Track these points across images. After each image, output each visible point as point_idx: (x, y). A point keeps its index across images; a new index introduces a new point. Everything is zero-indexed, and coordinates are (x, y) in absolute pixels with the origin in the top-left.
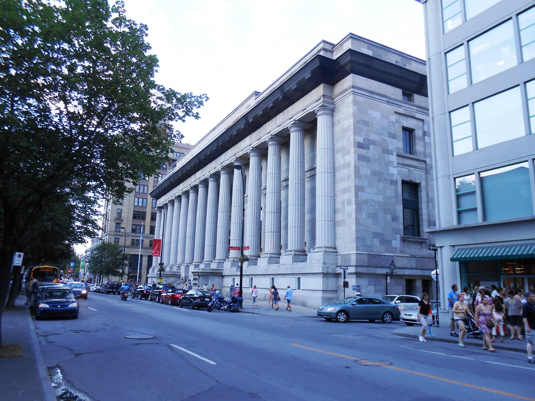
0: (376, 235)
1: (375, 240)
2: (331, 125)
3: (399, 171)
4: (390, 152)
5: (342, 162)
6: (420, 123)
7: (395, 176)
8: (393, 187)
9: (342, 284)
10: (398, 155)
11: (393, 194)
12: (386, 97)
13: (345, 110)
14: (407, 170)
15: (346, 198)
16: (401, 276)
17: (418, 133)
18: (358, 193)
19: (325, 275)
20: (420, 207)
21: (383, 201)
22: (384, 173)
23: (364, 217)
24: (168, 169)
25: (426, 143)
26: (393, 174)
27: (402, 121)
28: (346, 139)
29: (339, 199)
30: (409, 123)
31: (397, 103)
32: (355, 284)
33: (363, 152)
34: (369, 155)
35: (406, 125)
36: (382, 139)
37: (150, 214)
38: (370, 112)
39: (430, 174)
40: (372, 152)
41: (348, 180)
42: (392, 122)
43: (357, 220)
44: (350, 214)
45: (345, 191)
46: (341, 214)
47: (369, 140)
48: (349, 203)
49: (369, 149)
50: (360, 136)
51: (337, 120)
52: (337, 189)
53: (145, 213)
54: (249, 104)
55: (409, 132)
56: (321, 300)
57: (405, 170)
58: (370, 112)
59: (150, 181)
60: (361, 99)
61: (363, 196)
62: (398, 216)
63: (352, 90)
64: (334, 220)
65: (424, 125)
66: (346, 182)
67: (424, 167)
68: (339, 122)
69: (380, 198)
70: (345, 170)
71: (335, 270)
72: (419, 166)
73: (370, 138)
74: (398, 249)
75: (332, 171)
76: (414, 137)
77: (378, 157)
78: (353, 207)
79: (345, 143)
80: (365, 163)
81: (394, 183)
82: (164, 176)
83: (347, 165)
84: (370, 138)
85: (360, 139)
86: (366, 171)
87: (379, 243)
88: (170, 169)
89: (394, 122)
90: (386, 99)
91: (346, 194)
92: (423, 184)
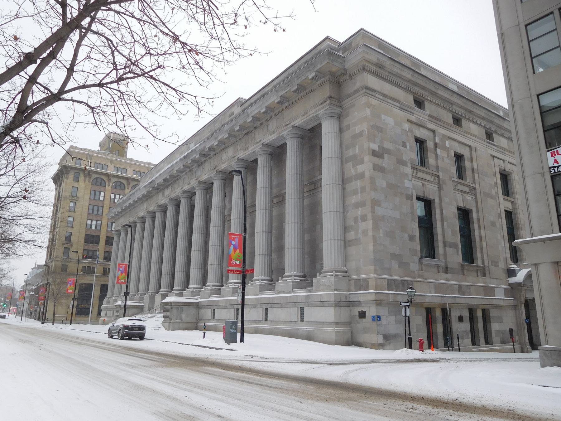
0: (394, 256)
1: (393, 261)
2: (338, 131)
3: (413, 185)
4: (404, 163)
5: (353, 172)
6: (431, 134)
7: (410, 190)
8: (409, 202)
9: (358, 314)
10: (412, 168)
13: (356, 113)
14: (421, 184)
15: (359, 213)
16: (421, 305)
17: (430, 145)
19: (338, 304)
20: (434, 226)
21: (399, 217)
22: (399, 186)
23: (381, 235)
24: (126, 189)
26: (409, 188)
28: (357, 147)
29: (351, 214)
30: (422, 133)
31: (409, 110)
32: (374, 315)
33: (378, 161)
34: (384, 165)
35: (418, 136)
36: (396, 148)
37: (105, 238)
38: (383, 117)
40: (387, 162)
41: (361, 193)
42: (405, 130)
44: (365, 232)
45: (358, 205)
46: (353, 233)
47: (383, 148)
48: (364, 218)
49: (384, 158)
50: (374, 142)
51: (346, 126)
52: (347, 203)
53: (99, 237)
54: (233, 111)
55: (421, 142)
56: (334, 333)
57: (419, 184)
58: (383, 117)
59: (105, 202)
60: (374, 101)
61: (380, 211)
62: (415, 236)
63: (364, 91)
65: (435, 136)
66: (359, 195)
67: (437, 182)
68: (348, 127)
69: (397, 215)
72: (432, 180)
73: (385, 146)
74: (416, 272)
77: (393, 168)
78: (369, 224)
79: (357, 151)
80: (380, 173)
81: (409, 197)
82: (121, 196)
83: (361, 176)
85: (374, 147)
86: (381, 183)
88: (128, 189)
89: (407, 130)
90: (399, 105)
91: (360, 209)
92: (437, 201)
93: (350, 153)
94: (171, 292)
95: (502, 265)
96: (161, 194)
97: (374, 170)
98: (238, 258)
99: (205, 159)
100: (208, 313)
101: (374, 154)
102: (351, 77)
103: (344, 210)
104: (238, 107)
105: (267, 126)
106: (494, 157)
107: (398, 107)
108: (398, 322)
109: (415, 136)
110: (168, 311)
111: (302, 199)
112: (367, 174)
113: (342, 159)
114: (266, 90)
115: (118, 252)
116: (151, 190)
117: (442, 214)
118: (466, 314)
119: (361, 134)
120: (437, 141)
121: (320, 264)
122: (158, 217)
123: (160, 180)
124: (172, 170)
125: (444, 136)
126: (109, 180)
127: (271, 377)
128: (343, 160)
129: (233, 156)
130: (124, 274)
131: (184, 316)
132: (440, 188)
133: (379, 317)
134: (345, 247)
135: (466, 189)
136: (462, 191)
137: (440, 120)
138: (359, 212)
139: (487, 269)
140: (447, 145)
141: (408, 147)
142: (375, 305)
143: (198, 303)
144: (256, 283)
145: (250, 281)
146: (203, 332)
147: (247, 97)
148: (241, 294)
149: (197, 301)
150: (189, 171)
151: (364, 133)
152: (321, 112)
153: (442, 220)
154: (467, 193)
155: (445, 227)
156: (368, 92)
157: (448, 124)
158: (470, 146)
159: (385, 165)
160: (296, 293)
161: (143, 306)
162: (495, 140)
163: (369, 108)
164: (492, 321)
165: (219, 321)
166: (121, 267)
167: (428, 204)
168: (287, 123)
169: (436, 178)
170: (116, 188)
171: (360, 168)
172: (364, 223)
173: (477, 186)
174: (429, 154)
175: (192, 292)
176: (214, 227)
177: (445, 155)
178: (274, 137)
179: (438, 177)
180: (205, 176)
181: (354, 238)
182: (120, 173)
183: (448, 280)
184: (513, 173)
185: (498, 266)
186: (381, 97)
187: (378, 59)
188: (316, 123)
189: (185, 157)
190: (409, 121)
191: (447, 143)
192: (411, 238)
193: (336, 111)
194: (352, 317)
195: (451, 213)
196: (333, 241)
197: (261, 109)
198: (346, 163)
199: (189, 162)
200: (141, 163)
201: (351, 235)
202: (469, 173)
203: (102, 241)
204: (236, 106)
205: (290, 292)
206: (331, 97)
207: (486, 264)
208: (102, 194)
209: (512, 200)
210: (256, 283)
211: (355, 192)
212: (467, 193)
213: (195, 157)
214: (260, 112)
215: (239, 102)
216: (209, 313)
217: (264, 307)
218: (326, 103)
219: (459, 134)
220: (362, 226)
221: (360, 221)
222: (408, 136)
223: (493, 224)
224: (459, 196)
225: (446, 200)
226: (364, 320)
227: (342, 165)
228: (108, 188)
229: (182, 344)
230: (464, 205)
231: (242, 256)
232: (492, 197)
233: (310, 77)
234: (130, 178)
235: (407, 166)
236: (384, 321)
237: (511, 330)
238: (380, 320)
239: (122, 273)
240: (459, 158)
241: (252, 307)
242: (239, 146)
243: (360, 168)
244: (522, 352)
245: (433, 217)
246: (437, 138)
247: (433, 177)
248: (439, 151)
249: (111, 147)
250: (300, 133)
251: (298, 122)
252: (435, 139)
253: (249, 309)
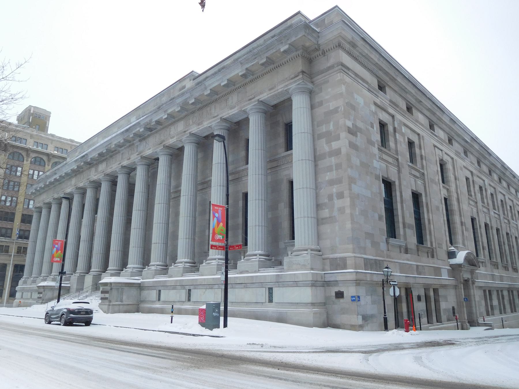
0: (369, 235)
1: (367, 240)
5: (327, 149)
6: (390, 118)
7: (378, 170)
8: (377, 181)
9: (334, 295)
10: (380, 150)
11: (378, 191)
12: (367, 83)
13: (330, 90)
15: (334, 190)
17: (390, 129)
18: (351, 185)
19: (314, 284)
21: (371, 197)
23: (357, 213)
24: (46, 166)
25: (397, 140)
27: (378, 112)
28: (332, 123)
29: (324, 192)
30: (385, 118)
31: (375, 92)
34: (357, 143)
35: (381, 119)
36: (366, 128)
37: (21, 215)
39: (402, 173)
40: (359, 141)
41: (336, 169)
43: (352, 215)
44: (341, 210)
45: (332, 183)
46: (327, 210)
48: (340, 196)
49: (357, 136)
50: (349, 120)
53: (13, 214)
54: (183, 85)
57: (384, 165)
58: (356, 96)
60: (348, 79)
61: (356, 189)
63: (340, 67)
64: (315, 216)
65: (394, 121)
66: (334, 172)
67: (397, 165)
68: (321, 104)
69: (368, 194)
70: (333, 158)
71: (323, 278)
72: (393, 163)
75: (313, 160)
76: (386, 132)
77: (364, 147)
78: (347, 201)
79: (331, 127)
83: (337, 153)
84: (357, 125)
85: (349, 124)
86: (356, 161)
87: (370, 245)
88: (48, 165)
90: (367, 86)
91: (335, 186)
92: (397, 183)
93: (324, 129)
94: (104, 272)
95: (445, 248)
96: (93, 170)
97: (350, 147)
98: (221, 232)
99: (149, 133)
101: (353, 132)
102: (324, 53)
103: (317, 187)
104: (191, 80)
106: (435, 146)
107: (366, 88)
108: (373, 302)
109: (379, 119)
110: (107, 292)
111: (266, 175)
112: (344, 151)
113: (313, 135)
114: (225, 64)
115: (38, 230)
116: (83, 165)
117: (401, 196)
118: (422, 293)
119: (336, 111)
120: (396, 126)
121: (284, 243)
122: (89, 194)
123: (95, 155)
124: (110, 144)
125: (400, 121)
126: (28, 155)
127: (398, 384)
128: (315, 137)
129: (184, 130)
130: (60, 252)
131: (124, 298)
132: (399, 171)
133: (359, 297)
134: (318, 225)
135: (417, 174)
136: (415, 176)
137: (397, 106)
138: (335, 189)
139: (435, 250)
140: (403, 131)
141: (375, 128)
142: (355, 284)
143: (140, 284)
144: (213, 262)
145: (173, 264)
146: (171, 315)
147: (200, 72)
148: (224, 273)
149: (139, 282)
150: (130, 146)
151: (340, 109)
152: (293, 86)
153: (402, 202)
154: (417, 177)
155: (404, 209)
156: (344, 69)
157: (403, 111)
158: (419, 135)
159: (358, 144)
160: (262, 273)
161: (70, 287)
162: (436, 131)
163: (344, 84)
164: (440, 300)
165: (165, 302)
166: (57, 244)
167: (388, 185)
168: (251, 97)
169: (396, 161)
170: (35, 164)
171: (335, 145)
172: (341, 201)
173: (426, 173)
174: (390, 137)
175: (131, 272)
176: (159, 203)
177: (402, 140)
178: (235, 111)
179: (397, 160)
180: (149, 151)
181: (328, 216)
182: (40, 149)
183: (408, 260)
184: (448, 163)
185: (442, 248)
186: (353, 76)
187: (353, 38)
188: (285, 98)
189: (127, 130)
190: (375, 104)
191: (404, 129)
192: (380, 218)
193: (308, 87)
194: (327, 298)
195: (408, 196)
196: (306, 219)
197: (222, 82)
198: (319, 139)
199: (131, 136)
200: (63, 140)
201: (325, 213)
202: (418, 159)
203: (18, 218)
204: (188, 80)
205: (255, 272)
206: (303, 72)
207: (434, 246)
208: (19, 169)
209: (448, 187)
210: (213, 262)
211: (330, 169)
212: (417, 177)
213: (139, 130)
214: (220, 84)
215: (192, 76)
216: (153, 294)
218: (298, 78)
219: (410, 121)
220: (338, 203)
221: (336, 198)
222: (374, 117)
223: (438, 208)
224: (412, 180)
225: (404, 183)
226: (342, 300)
227: (314, 141)
228: (27, 163)
229: (145, 330)
230: (416, 189)
231: (225, 230)
232: (435, 183)
233: (282, 50)
234: (51, 154)
235: (374, 146)
236: (362, 302)
237: (453, 308)
238: (359, 301)
239: (57, 251)
240: (411, 144)
241: (208, 288)
242: (191, 121)
243: (335, 145)
244: (463, 329)
245: (394, 198)
246: (396, 123)
247: (394, 160)
248: (397, 135)
249: (30, 121)
250: (265, 109)
251: (264, 97)
252: (394, 124)
253: (204, 290)
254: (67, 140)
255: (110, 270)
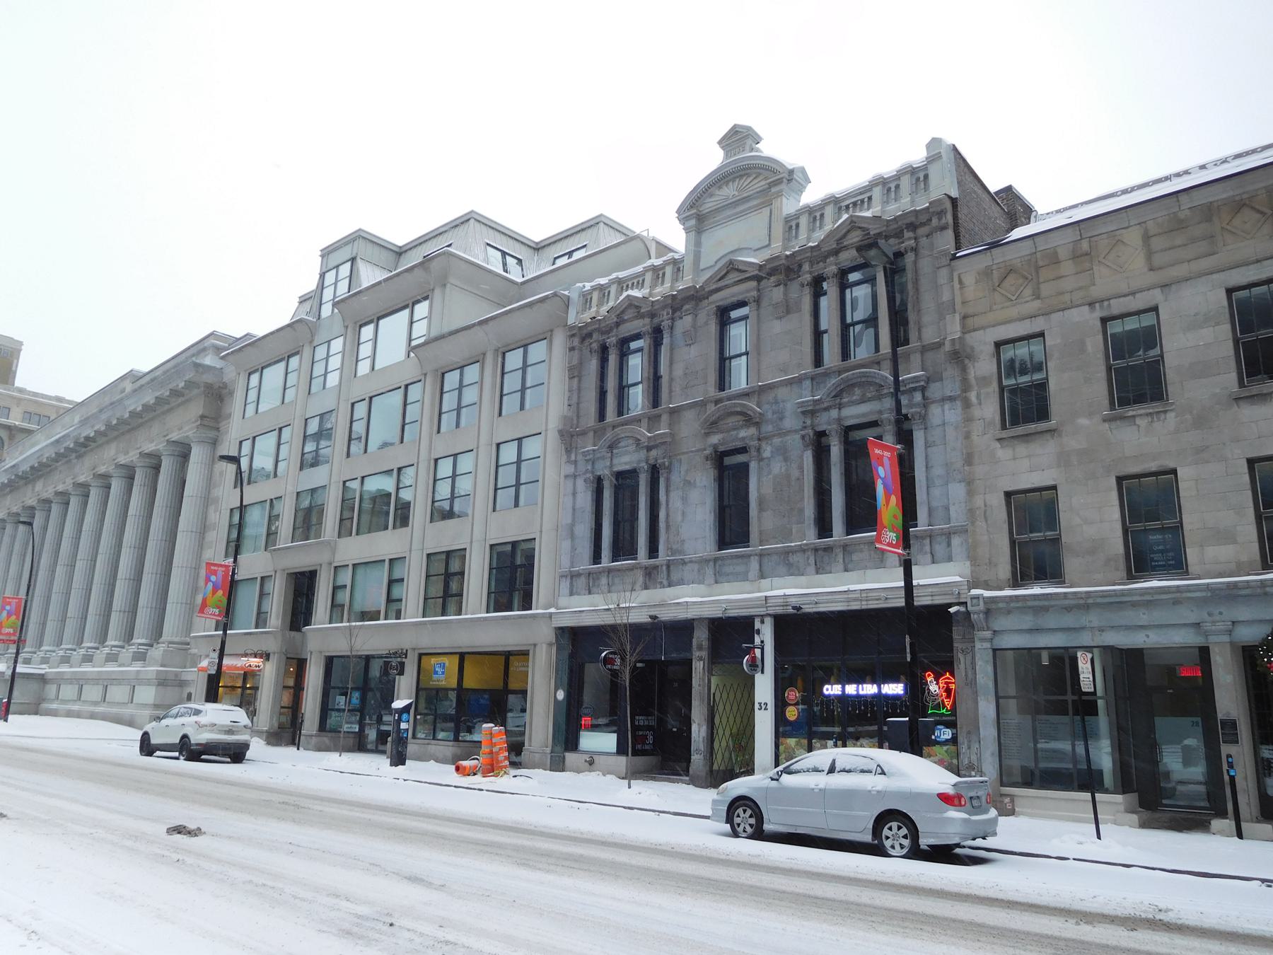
96: (30, 487)
99: (84, 449)
100: (51, 690)
105: (151, 427)
114: (157, 374)
123: (26, 467)
124: (42, 455)
143: (43, 675)
147: (146, 369)
150: (67, 462)
189: (57, 441)
193: (210, 435)
204: (128, 381)
205: (128, 666)
206: (202, 417)
215: (132, 376)
217: (105, 684)
234: (16, 427)
254: (50, 398)
255: (26, 652)
